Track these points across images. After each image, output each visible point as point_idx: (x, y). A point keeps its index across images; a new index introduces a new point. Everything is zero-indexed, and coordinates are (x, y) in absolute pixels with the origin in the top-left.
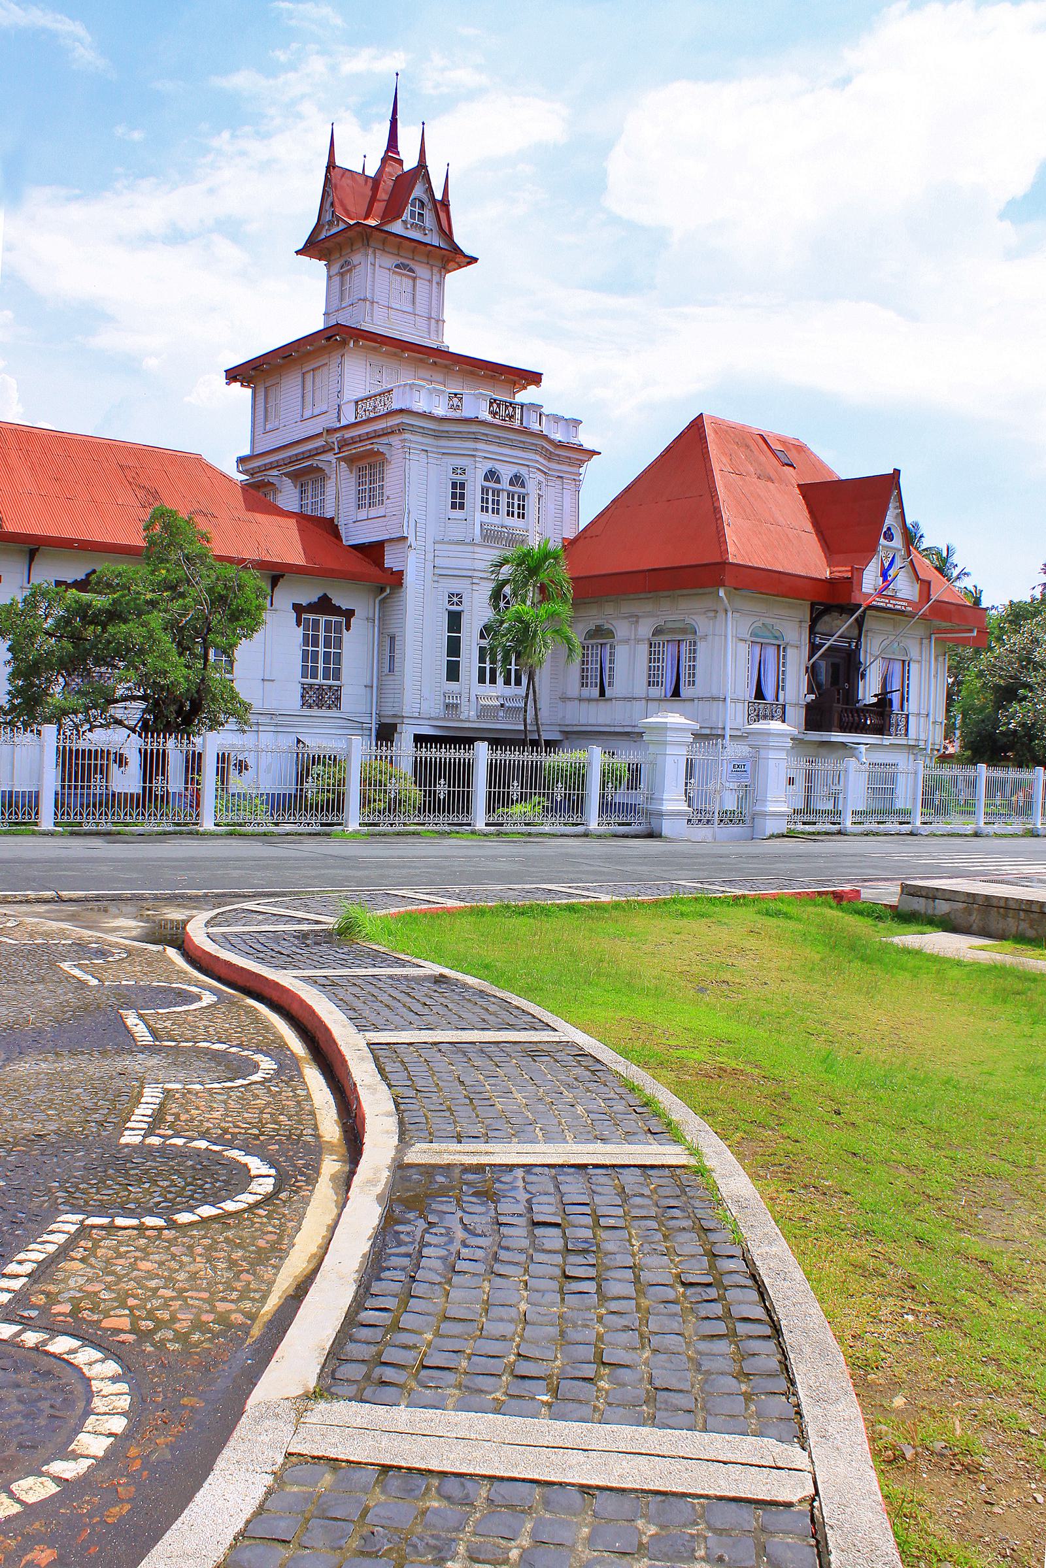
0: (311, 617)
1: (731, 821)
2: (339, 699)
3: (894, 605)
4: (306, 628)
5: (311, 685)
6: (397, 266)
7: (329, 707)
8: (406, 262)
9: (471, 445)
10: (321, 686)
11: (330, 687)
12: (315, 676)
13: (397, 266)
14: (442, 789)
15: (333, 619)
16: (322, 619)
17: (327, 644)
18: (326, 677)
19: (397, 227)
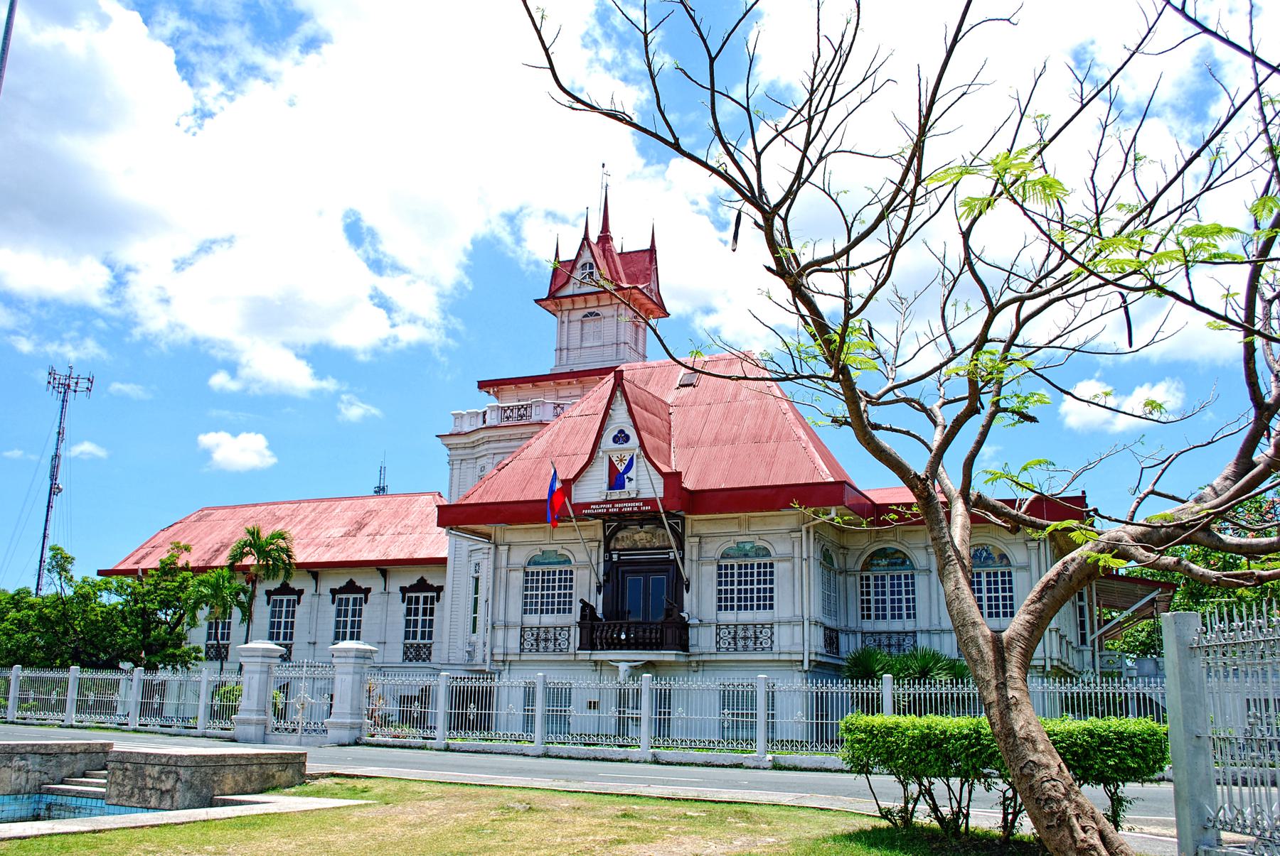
0: (414, 595)
1: (315, 731)
2: (430, 653)
3: (622, 508)
4: (410, 603)
5: (412, 645)
6: (584, 317)
7: (424, 660)
8: (592, 310)
9: (486, 446)
10: (418, 645)
11: (425, 645)
12: (415, 638)
13: (585, 316)
14: (92, 697)
15: (429, 594)
16: (422, 595)
17: (424, 614)
18: (423, 638)
19: (569, 290)
